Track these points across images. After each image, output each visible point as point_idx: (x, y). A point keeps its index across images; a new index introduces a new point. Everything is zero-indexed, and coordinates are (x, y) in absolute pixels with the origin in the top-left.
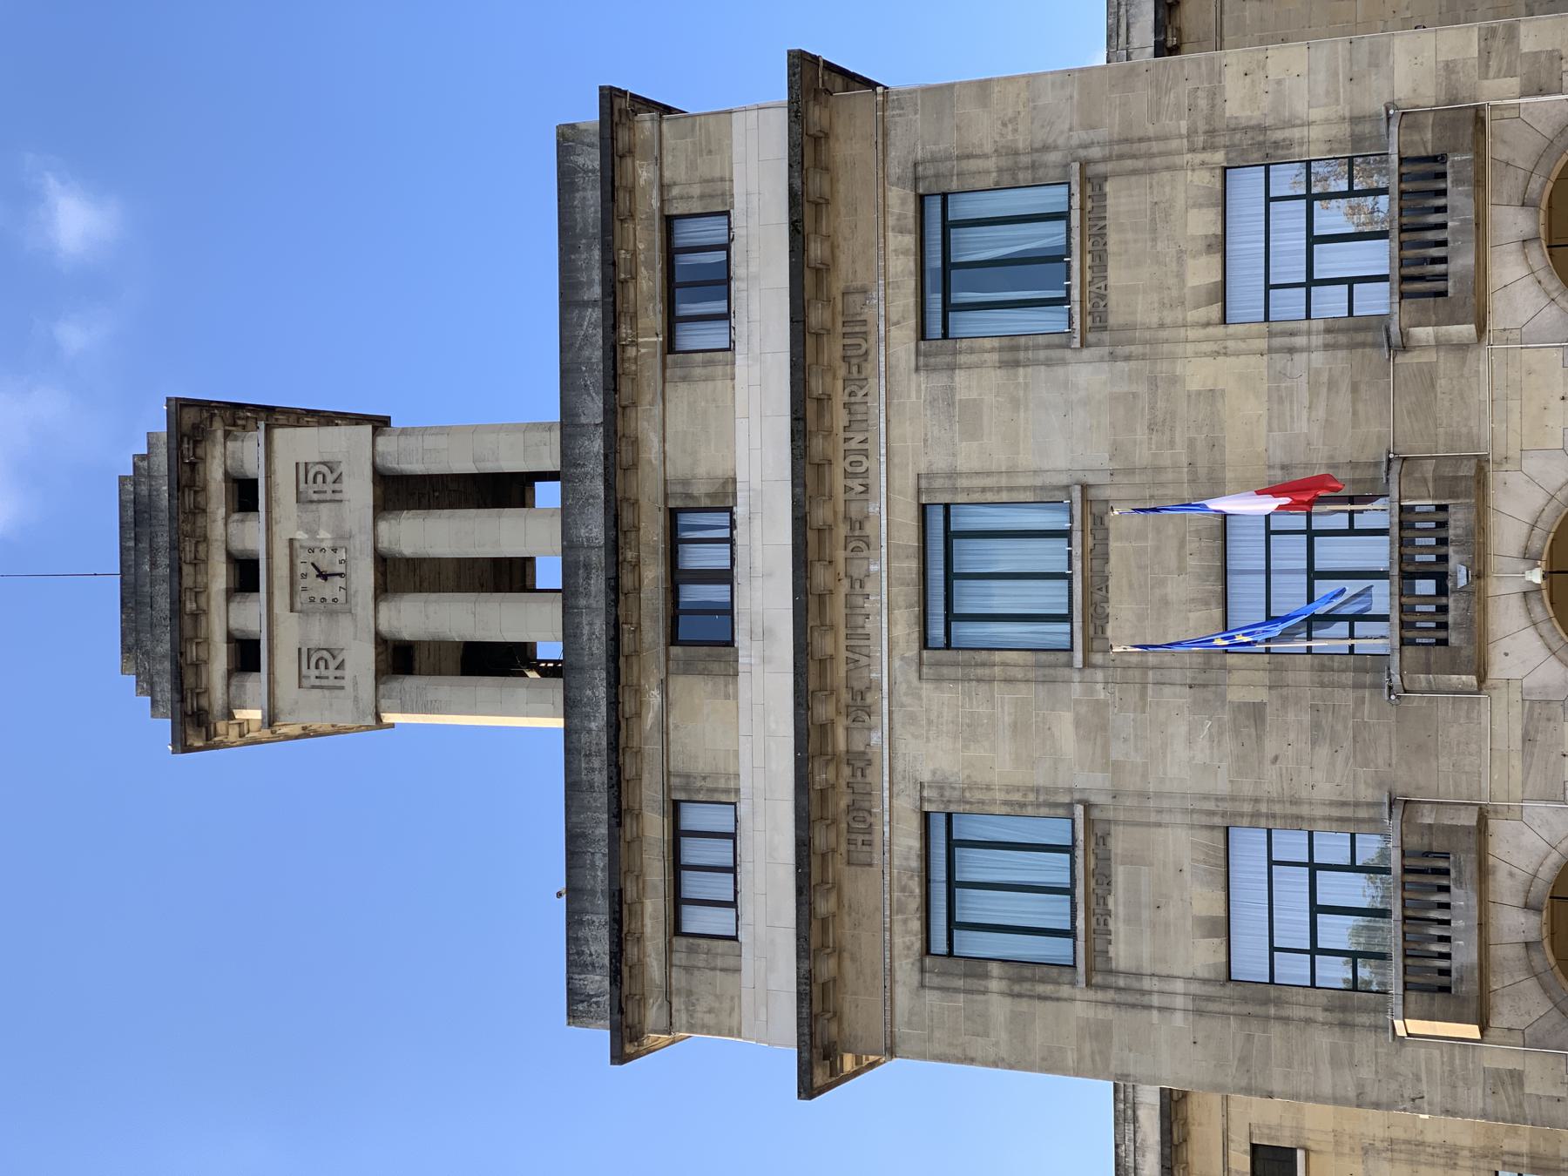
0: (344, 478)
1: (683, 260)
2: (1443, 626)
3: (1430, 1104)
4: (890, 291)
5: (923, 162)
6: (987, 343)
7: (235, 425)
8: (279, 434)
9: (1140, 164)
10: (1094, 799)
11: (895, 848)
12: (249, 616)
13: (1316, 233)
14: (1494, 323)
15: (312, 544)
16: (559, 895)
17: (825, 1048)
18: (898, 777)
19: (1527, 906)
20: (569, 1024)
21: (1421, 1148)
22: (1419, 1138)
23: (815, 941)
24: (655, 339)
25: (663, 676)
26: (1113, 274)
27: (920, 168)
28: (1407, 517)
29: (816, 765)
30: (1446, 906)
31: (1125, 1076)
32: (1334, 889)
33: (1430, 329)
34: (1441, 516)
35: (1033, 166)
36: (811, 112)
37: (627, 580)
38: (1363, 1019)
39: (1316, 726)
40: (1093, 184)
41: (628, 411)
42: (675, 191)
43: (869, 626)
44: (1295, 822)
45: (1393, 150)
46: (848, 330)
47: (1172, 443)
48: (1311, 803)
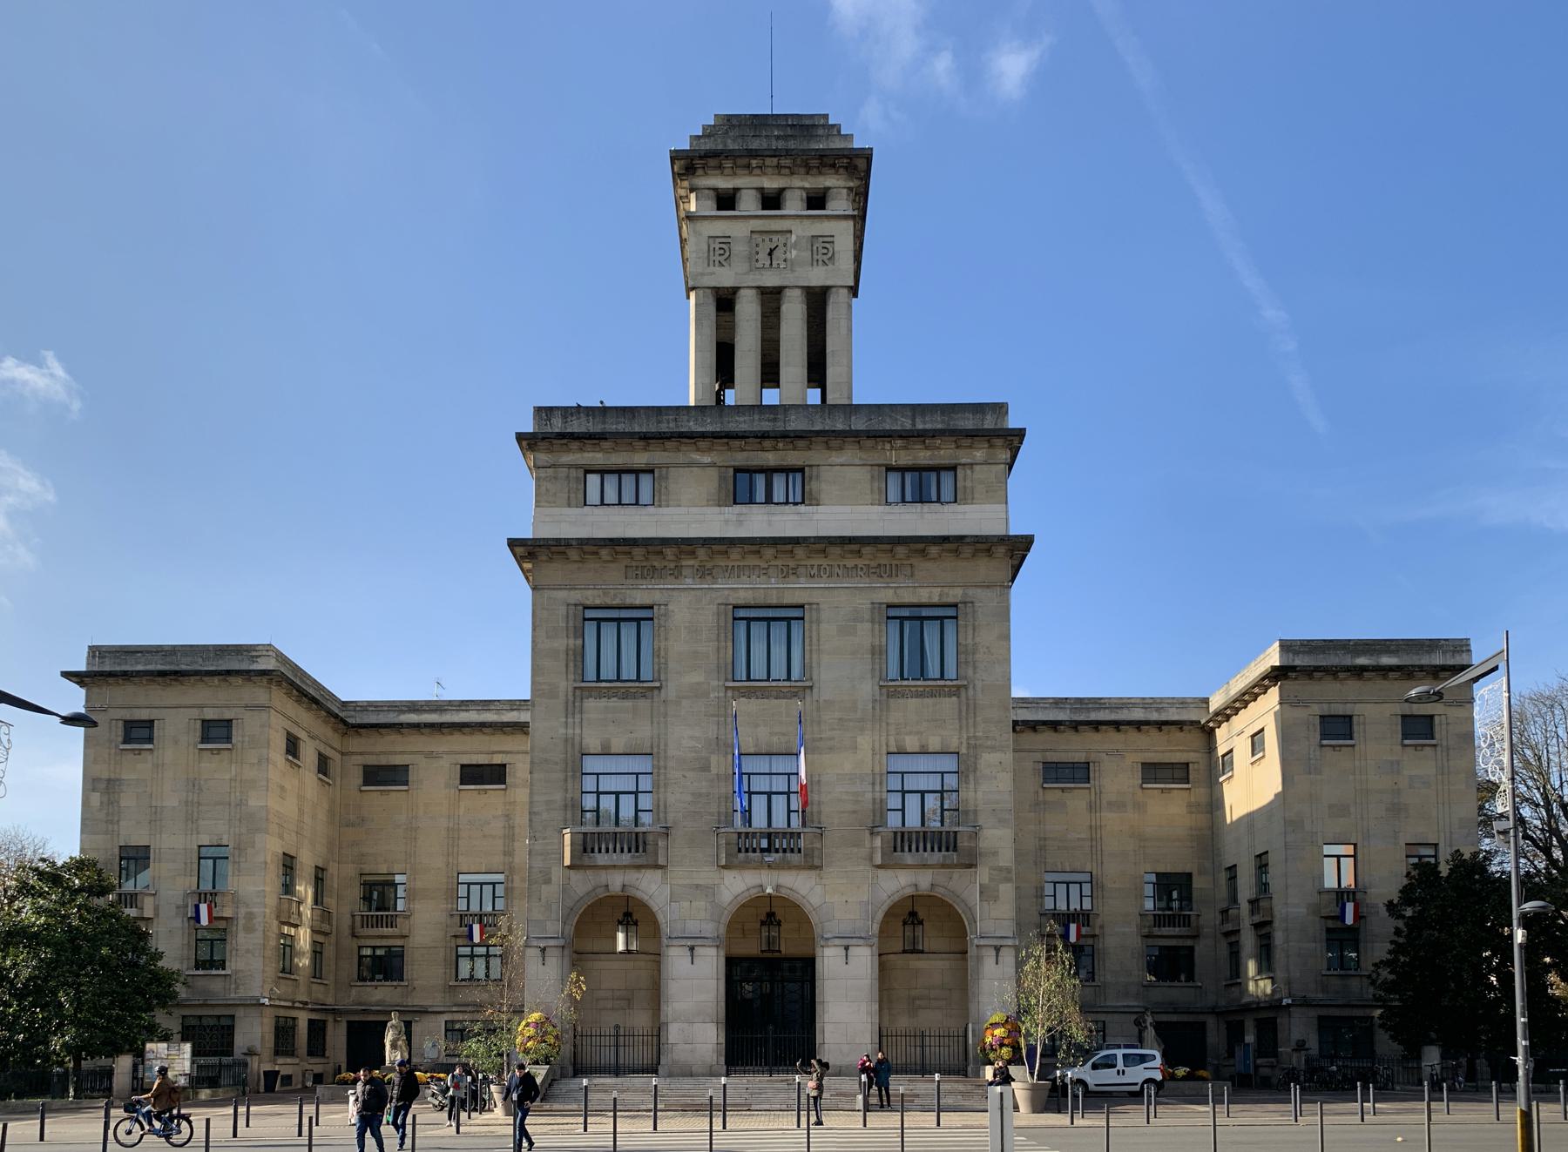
0: (826, 267)
1: (933, 476)
2: (747, 851)
3: (533, 844)
4: (911, 589)
5: (973, 606)
6: (884, 639)
7: (856, 194)
8: (851, 223)
9: (964, 714)
10: (663, 691)
11: (635, 591)
12: (749, 204)
13: (926, 795)
14: (880, 871)
15: (788, 245)
16: (602, 402)
17: (534, 553)
18: (670, 592)
19: (624, 886)
20: (534, 407)
23: (586, 548)
24: (894, 460)
25: (718, 464)
26: (914, 700)
27: (970, 605)
28: (796, 838)
29: (674, 549)
30: (622, 851)
31: (533, 705)
32: (627, 804)
33: (879, 845)
34: (796, 850)
35: (967, 662)
36: (1002, 547)
37: (767, 443)
38: (569, 815)
39: (700, 795)
40: (956, 691)
41: (857, 444)
42: (969, 472)
43: (744, 578)
44: (656, 784)
45: (961, 829)
46: (894, 566)
47: (834, 729)
48: (665, 792)
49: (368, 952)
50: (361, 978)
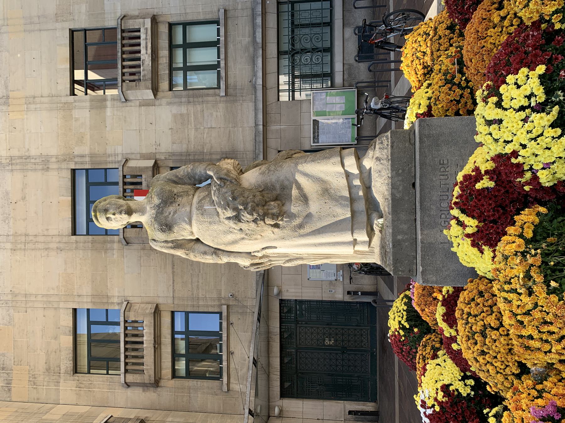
21: (28, 160)
22: (27, 154)
49: (181, 365)
50: (217, 376)
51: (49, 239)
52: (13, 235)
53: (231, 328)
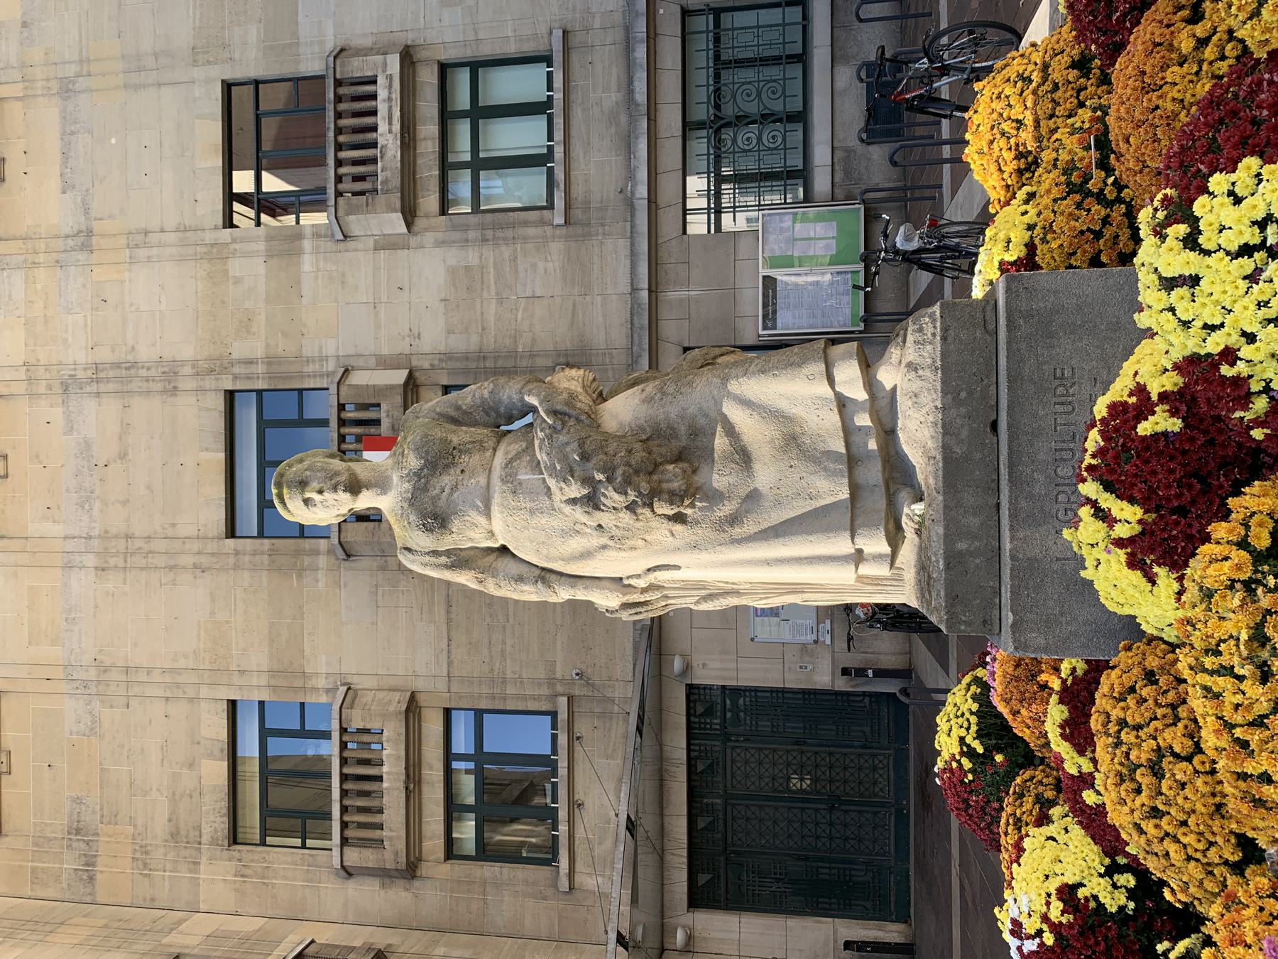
21: (133, 372)
22: (130, 358)
49: (467, 830)
50: (546, 855)
51: (177, 545)
52: (99, 537)
53: (578, 748)
